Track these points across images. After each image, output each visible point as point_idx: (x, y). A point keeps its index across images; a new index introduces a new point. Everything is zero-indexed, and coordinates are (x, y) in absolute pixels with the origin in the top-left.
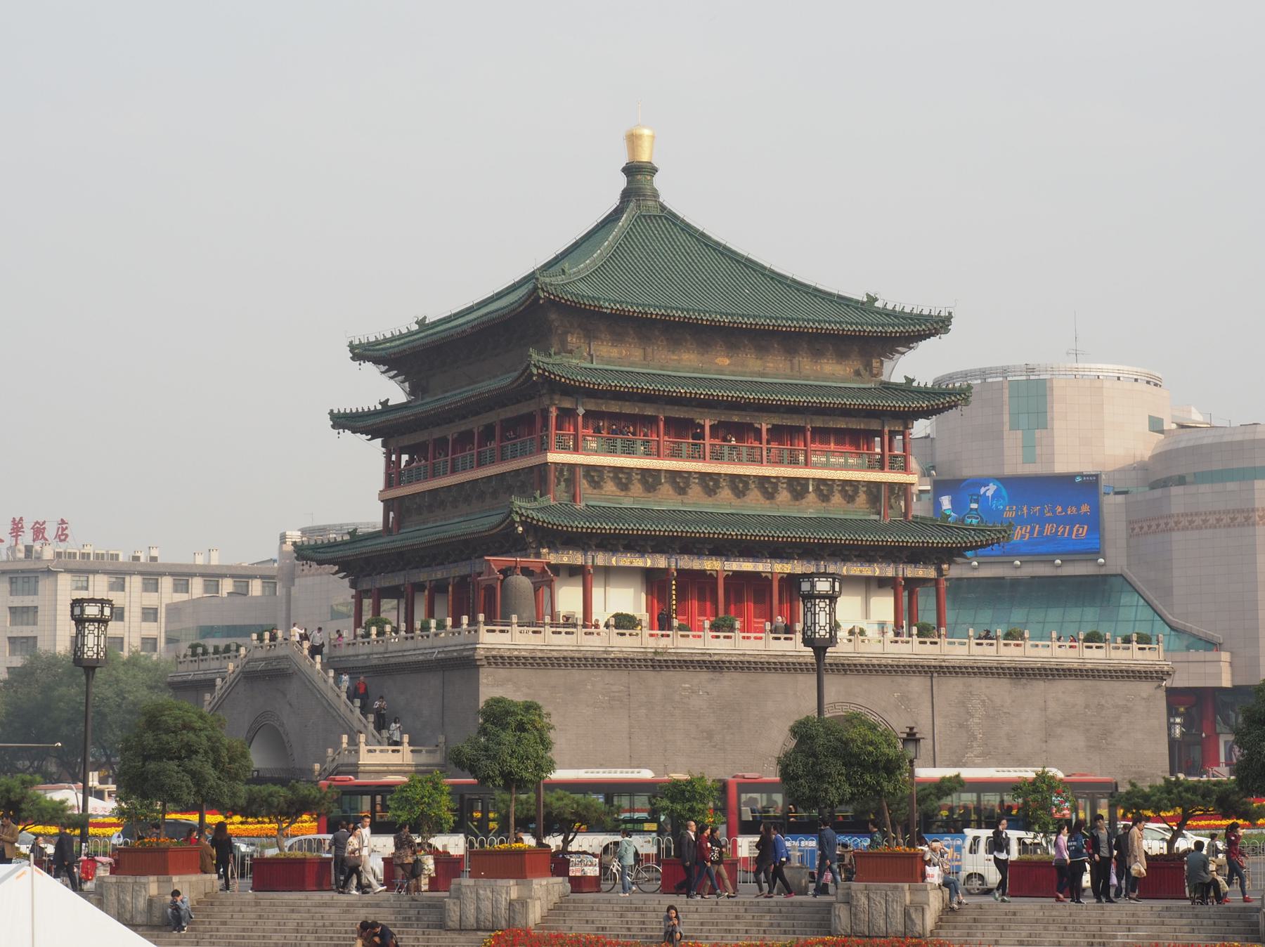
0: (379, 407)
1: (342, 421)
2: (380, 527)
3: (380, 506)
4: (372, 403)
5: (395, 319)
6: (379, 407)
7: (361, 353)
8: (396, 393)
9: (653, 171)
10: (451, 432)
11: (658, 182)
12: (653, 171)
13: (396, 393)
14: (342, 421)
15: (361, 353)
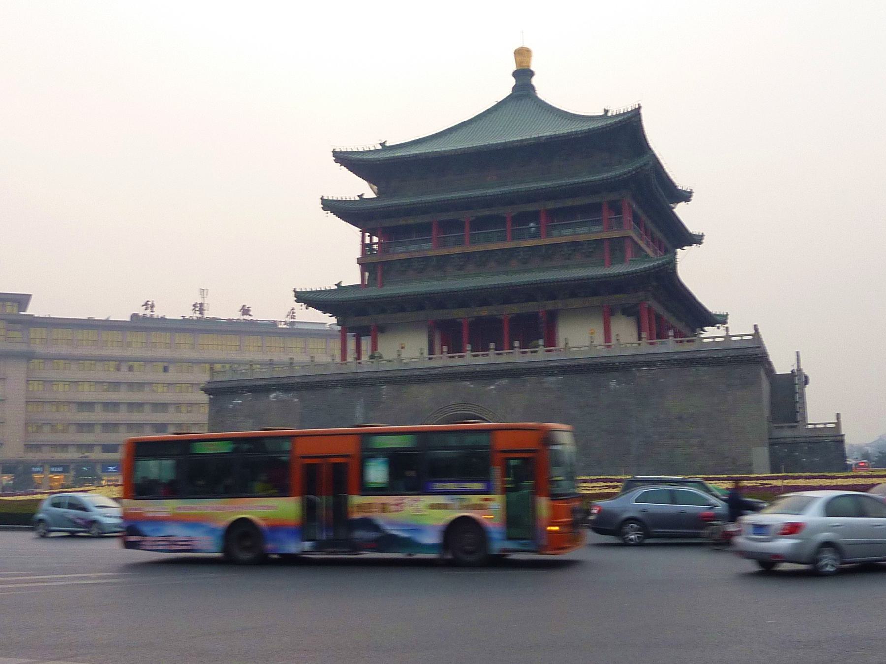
0: (358, 198)
1: (330, 206)
2: (358, 281)
3: (357, 268)
4: (353, 196)
5: (365, 141)
6: (358, 198)
7: (342, 158)
8: (367, 191)
9: (532, 74)
10: (467, 216)
11: (534, 81)
12: (532, 74)
13: (367, 191)
14: (330, 206)
15: (342, 158)
